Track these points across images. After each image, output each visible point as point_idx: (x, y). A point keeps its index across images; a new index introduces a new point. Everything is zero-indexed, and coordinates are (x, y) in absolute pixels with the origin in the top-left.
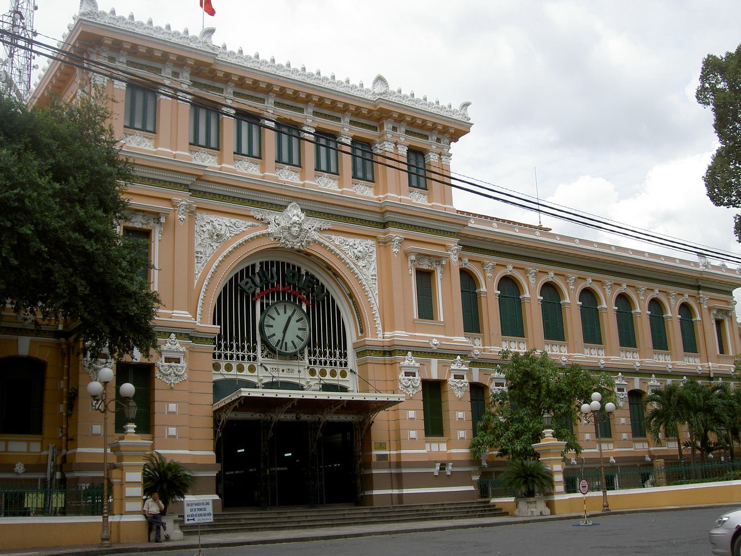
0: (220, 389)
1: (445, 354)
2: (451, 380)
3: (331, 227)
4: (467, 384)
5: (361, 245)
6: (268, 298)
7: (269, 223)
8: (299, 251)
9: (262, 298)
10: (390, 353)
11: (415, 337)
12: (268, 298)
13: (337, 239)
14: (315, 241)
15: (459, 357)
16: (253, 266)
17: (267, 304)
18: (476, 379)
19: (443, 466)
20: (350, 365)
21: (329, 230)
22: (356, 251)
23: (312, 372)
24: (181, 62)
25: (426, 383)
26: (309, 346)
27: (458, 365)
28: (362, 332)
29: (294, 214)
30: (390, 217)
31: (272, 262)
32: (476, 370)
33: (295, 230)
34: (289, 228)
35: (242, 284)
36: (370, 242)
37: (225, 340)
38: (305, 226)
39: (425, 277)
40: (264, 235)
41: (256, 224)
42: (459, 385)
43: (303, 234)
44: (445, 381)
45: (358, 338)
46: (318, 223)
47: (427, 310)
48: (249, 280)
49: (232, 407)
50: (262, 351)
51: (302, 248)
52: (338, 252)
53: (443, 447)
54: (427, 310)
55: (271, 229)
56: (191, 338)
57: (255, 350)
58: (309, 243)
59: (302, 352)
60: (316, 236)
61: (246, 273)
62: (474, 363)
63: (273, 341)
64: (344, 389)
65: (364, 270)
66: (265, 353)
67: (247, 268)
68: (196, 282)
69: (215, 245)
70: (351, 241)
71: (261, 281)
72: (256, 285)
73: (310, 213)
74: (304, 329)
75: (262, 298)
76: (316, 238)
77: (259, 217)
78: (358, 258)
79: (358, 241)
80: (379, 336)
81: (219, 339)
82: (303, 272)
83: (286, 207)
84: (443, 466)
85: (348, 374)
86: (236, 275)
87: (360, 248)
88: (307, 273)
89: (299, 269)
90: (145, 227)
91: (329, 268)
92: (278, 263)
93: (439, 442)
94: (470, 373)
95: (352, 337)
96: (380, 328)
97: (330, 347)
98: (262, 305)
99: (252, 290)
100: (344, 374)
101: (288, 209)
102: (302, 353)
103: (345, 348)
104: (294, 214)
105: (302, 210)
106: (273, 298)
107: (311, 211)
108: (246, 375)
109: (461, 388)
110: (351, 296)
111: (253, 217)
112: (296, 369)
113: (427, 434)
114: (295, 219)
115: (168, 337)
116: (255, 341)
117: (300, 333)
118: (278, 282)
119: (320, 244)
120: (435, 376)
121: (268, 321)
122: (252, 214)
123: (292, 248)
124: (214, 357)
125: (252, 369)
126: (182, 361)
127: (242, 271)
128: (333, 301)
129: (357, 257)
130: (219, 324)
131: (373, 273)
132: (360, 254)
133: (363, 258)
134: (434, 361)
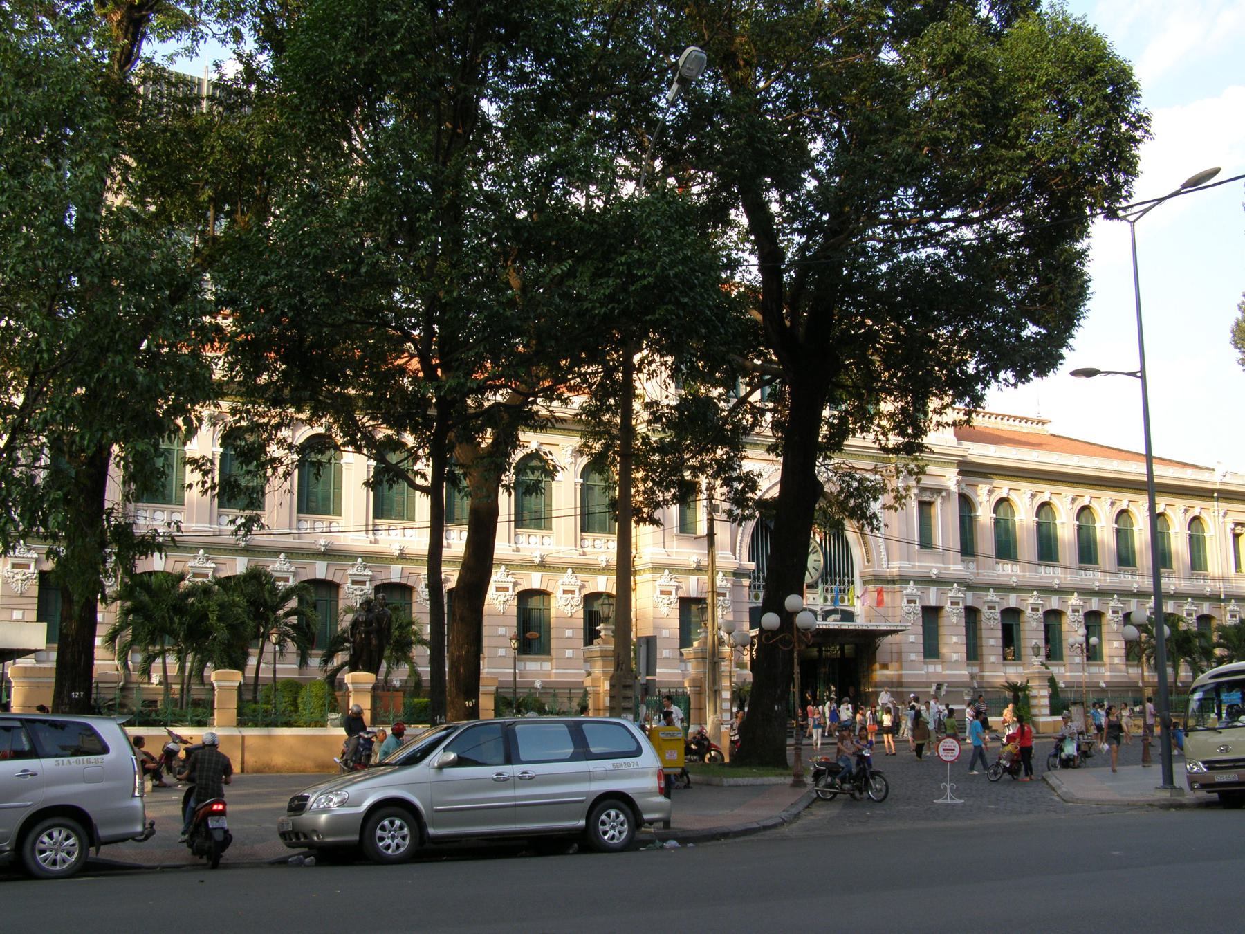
1: (942, 582)
2: (948, 606)
11: (914, 567)
18: (969, 604)
19: (939, 686)
27: (954, 592)
28: (868, 561)
32: (970, 594)
44: (942, 608)
45: (866, 567)
53: (939, 668)
59: (816, 583)
84: (939, 686)
93: (935, 664)
94: (964, 599)
96: (885, 559)
113: (925, 657)
120: (933, 603)
134: (933, 590)
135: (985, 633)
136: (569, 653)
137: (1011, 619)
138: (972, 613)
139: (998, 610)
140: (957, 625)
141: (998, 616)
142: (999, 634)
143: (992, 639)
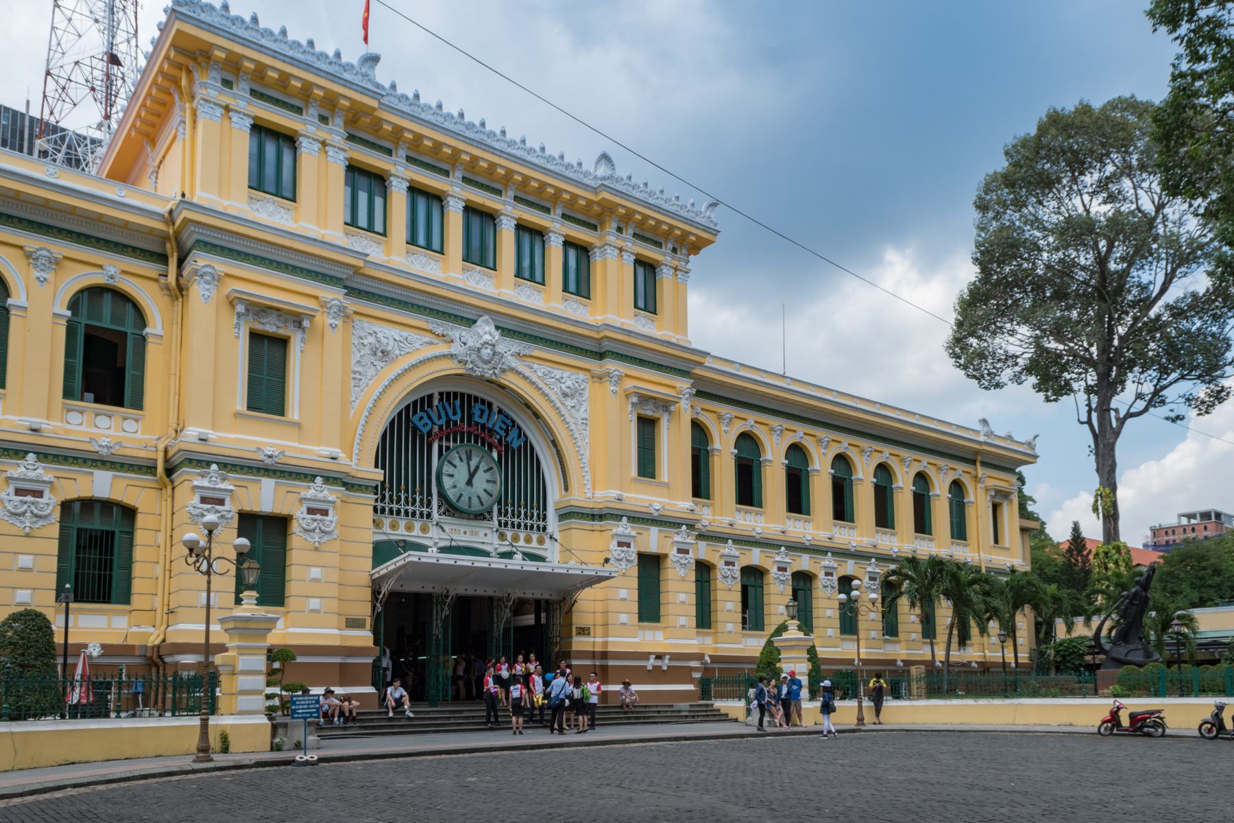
0: (382, 552)
3: (533, 354)
4: (693, 561)
5: (570, 379)
6: (448, 440)
7: (452, 341)
8: (490, 381)
9: (441, 440)
10: (601, 517)
12: (448, 440)
13: (542, 368)
14: (512, 369)
15: (684, 527)
16: (430, 397)
17: (448, 448)
18: (702, 556)
20: (550, 530)
22: (563, 386)
23: (502, 537)
25: (641, 556)
26: (500, 503)
28: (566, 489)
29: (486, 331)
30: (607, 346)
31: (455, 394)
32: (702, 544)
33: (486, 352)
34: (479, 350)
35: (415, 419)
36: (582, 376)
37: (391, 489)
38: (500, 349)
39: (647, 426)
40: (445, 356)
41: (435, 341)
42: (683, 561)
43: (496, 359)
44: (666, 556)
45: (562, 497)
46: (515, 346)
47: (647, 466)
48: (424, 415)
49: (396, 576)
50: (439, 507)
52: (541, 385)
54: (647, 466)
55: (456, 349)
56: (345, 484)
57: (429, 504)
58: (503, 371)
61: (419, 404)
62: (701, 537)
63: (452, 494)
64: (542, 559)
65: (573, 411)
66: (443, 509)
67: (422, 399)
68: (352, 412)
69: (382, 364)
70: (558, 373)
71: (440, 417)
72: (433, 423)
73: (506, 332)
74: (495, 482)
75: (441, 440)
76: (513, 365)
77: (439, 331)
78: (565, 395)
79: (567, 373)
80: (586, 493)
81: (383, 489)
82: (495, 409)
83: (475, 322)
85: (547, 540)
86: (407, 407)
87: (569, 383)
88: (500, 411)
89: (490, 405)
91: (528, 406)
92: (462, 395)
95: (554, 494)
97: (526, 507)
98: (440, 448)
99: (428, 428)
100: (541, 541)
101: (478, 323)
102: (490, 513)
103: (545, 509)
104: (486, 331)
105: (497, 328)
106: (455, 441)
107: (509, 330)
108: (416, 535)
110: (555, 443)
111: (431, 331)
112: (482, 532)
114: (487, 337)
115: (313, 481)
116: (430, 494)
117: (490, 487)
118: (462, 420)
119: (519, 373)
121: (447, 469)
122: (430, 327)
123: (482, 376)
124: (375, 510)
125: (424, 529)
126: (331, 512)
127: (415, 403)
128: (532, 448)
130: (384, 468)
131: (584, 416)
132: (568, 391)
133: (572, 396)
134: (654, 530)
135: (720, 595)
136: (314, 603)
137: (753, 577)
138: (704, 569)
139: (737, 568)
140: (683, 580)
141: (738, 574)
142: (738, 596)
143: (728, 601)
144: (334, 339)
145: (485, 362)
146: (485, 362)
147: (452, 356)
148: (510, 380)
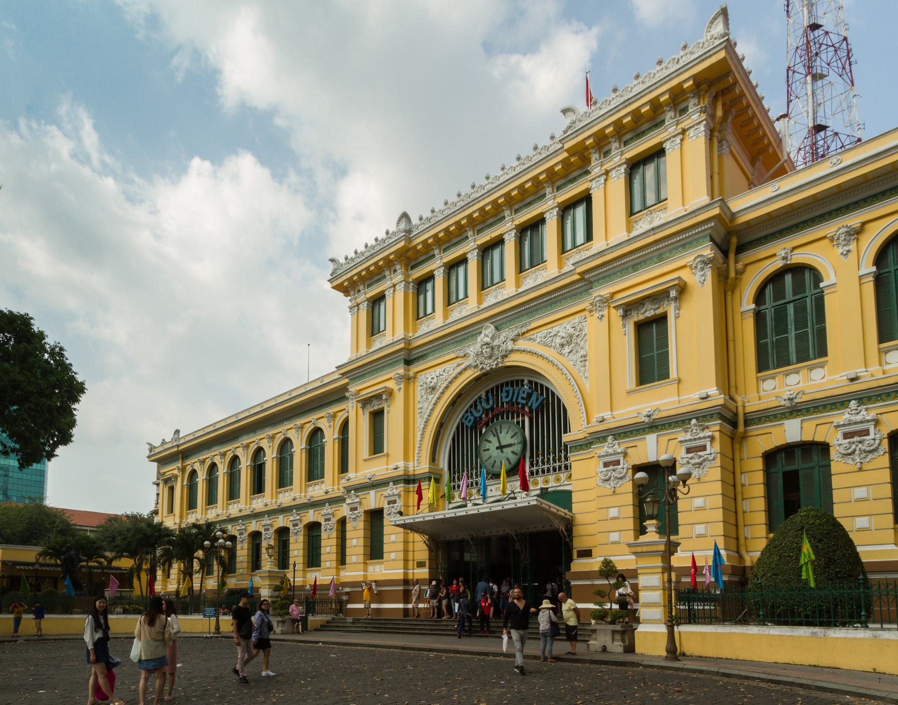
14: (512, 351)
21: (528, 331)
24: (389, 263)
38: (496, 343)
40: (465, 369)
51: (500, 365)
55: (470, 361)
60: (510, 345)
76: (510, 348)
90: (381, 406)
109: (701, 464)
119: (518, 350)
129: (536, 350)
134: (651, 438)
144: (399, 397)
145: (490, 357)
146: (490, 357)
147: (469, 366)
148: (515, 360)
